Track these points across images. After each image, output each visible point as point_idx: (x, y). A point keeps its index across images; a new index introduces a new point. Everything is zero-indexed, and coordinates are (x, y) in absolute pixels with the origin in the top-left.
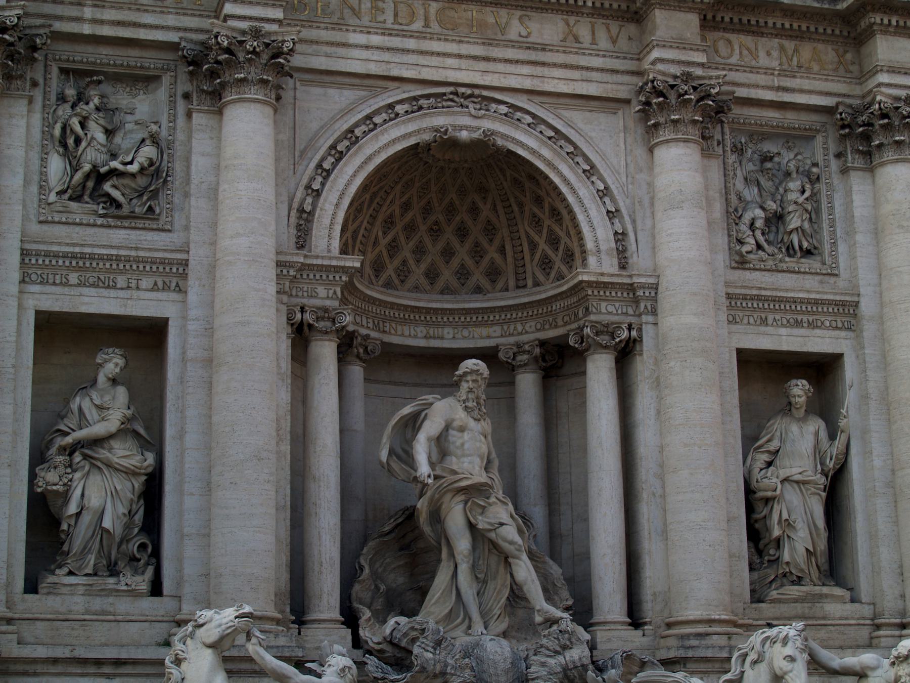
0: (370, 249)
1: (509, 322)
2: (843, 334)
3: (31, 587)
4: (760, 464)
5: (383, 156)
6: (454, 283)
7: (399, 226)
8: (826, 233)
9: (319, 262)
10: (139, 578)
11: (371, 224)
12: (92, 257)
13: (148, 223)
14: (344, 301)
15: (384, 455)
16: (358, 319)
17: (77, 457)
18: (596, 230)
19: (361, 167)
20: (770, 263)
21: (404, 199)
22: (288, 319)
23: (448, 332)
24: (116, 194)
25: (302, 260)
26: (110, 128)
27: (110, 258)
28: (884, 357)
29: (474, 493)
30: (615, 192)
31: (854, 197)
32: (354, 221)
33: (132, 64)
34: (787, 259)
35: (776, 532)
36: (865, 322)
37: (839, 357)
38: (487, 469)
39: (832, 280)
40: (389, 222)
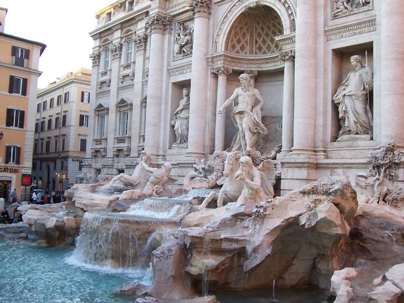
2: (374, 33)
5: (234, 19)
7: (263, 35)
16: (249, 66)
18: (286, 22)
19: (229, 25)
20: (347, 14)
21: (260, 26)
24: (185, 50)
25: (210, 56)
26: (185, 34)
30: (291, 7)
33: (187, 16)
35: (340, 116)
37: (372, 42)
39: (371, 11)
40: (259, 35)
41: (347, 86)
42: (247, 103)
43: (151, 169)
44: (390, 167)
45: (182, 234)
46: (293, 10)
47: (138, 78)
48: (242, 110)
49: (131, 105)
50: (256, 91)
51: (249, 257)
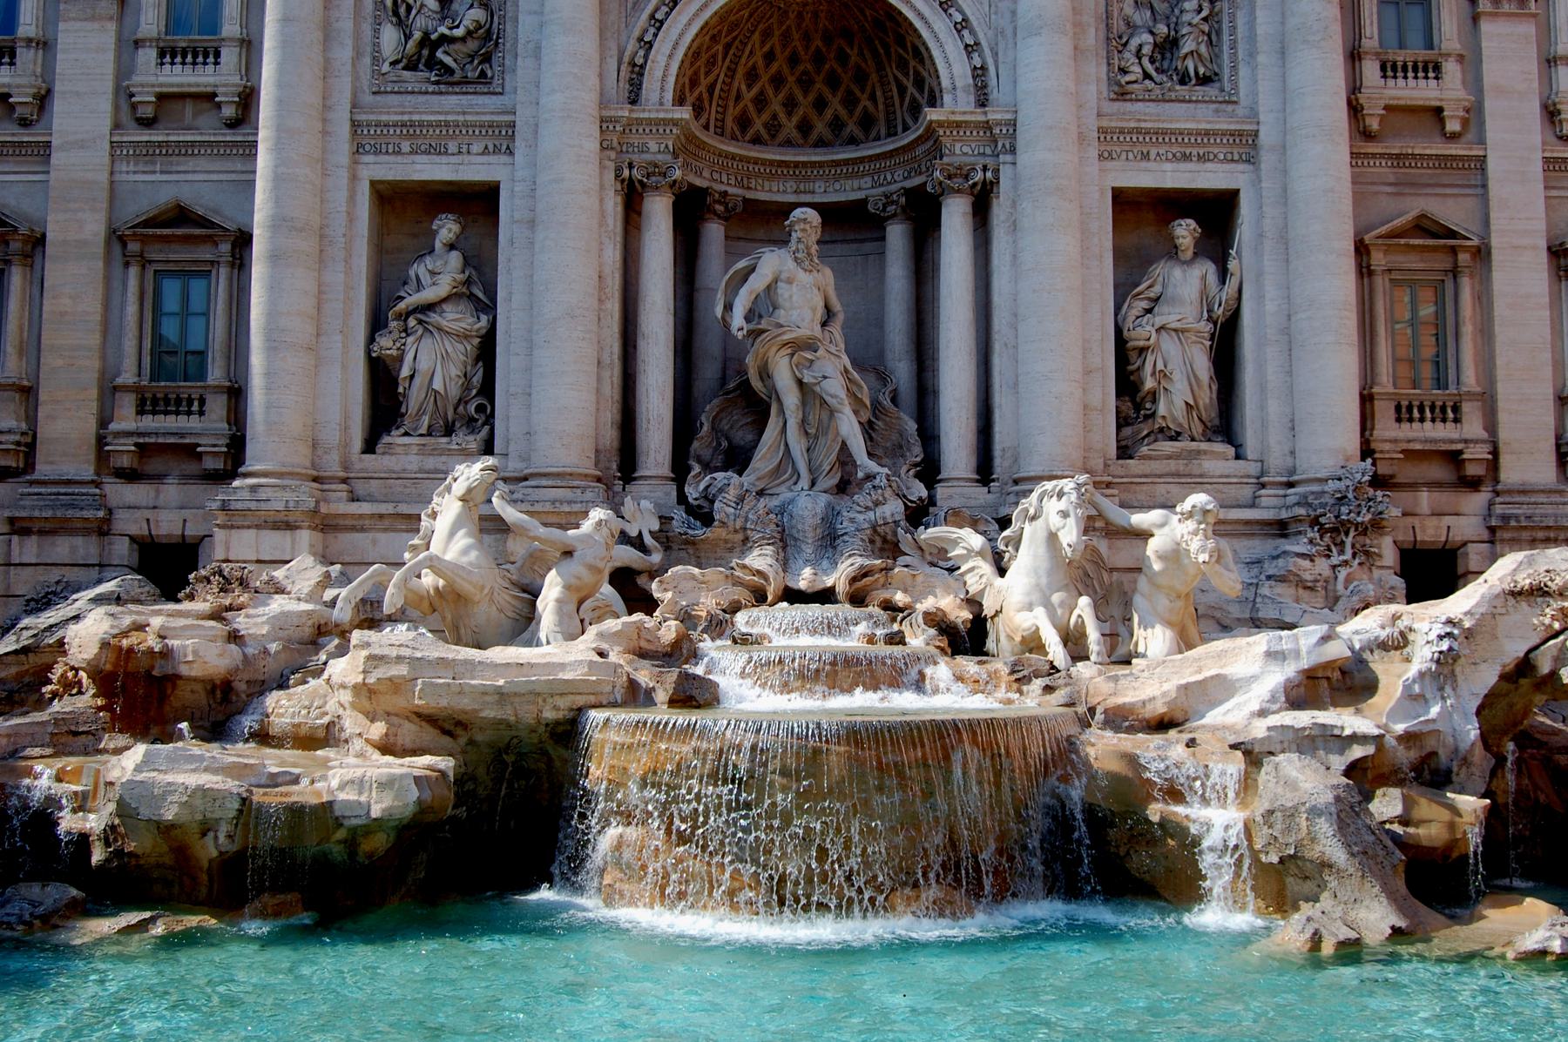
0: (731, 104)
1: (879, 172)
2: (1241, 167)
3: (370, 447)
4: (1135, 312)
6: (828, 135)
7: (765, 78)
8: (1226, 57)
9: (646, 115)
10: (471, 438)
11: (732, 77)
12: (421, 124)
13: (480, 88)
14: (675, 155)
15: (719, 311)
16: (716, 176)
17: (412, 322)
18: (951, 65)
19: (696, 15)
21: (765, 49)
22: (617, 176)
23: (819, 186)
24: (448, 60)
27: (439, 124)
28: (1285, 190)
29: (797, 346)
31: (1259, 13)
32: (707, 74)
34: (1178, 87)
35: (1149, 384)
36: (1262, 153)
37: (1236, 192)
38: (824, 324)
39: (1230, 108)
40: (752, 76)
41: (1156, 300)
42: (814, 310)
43: (556, 533)
44: (1364, 533)
45: (1291, 736)
46: (981, 36)
47: (82, 119)
48: (809, 333)
49: (40, 241)
50: (828, 272)
51: (1454, 778)
